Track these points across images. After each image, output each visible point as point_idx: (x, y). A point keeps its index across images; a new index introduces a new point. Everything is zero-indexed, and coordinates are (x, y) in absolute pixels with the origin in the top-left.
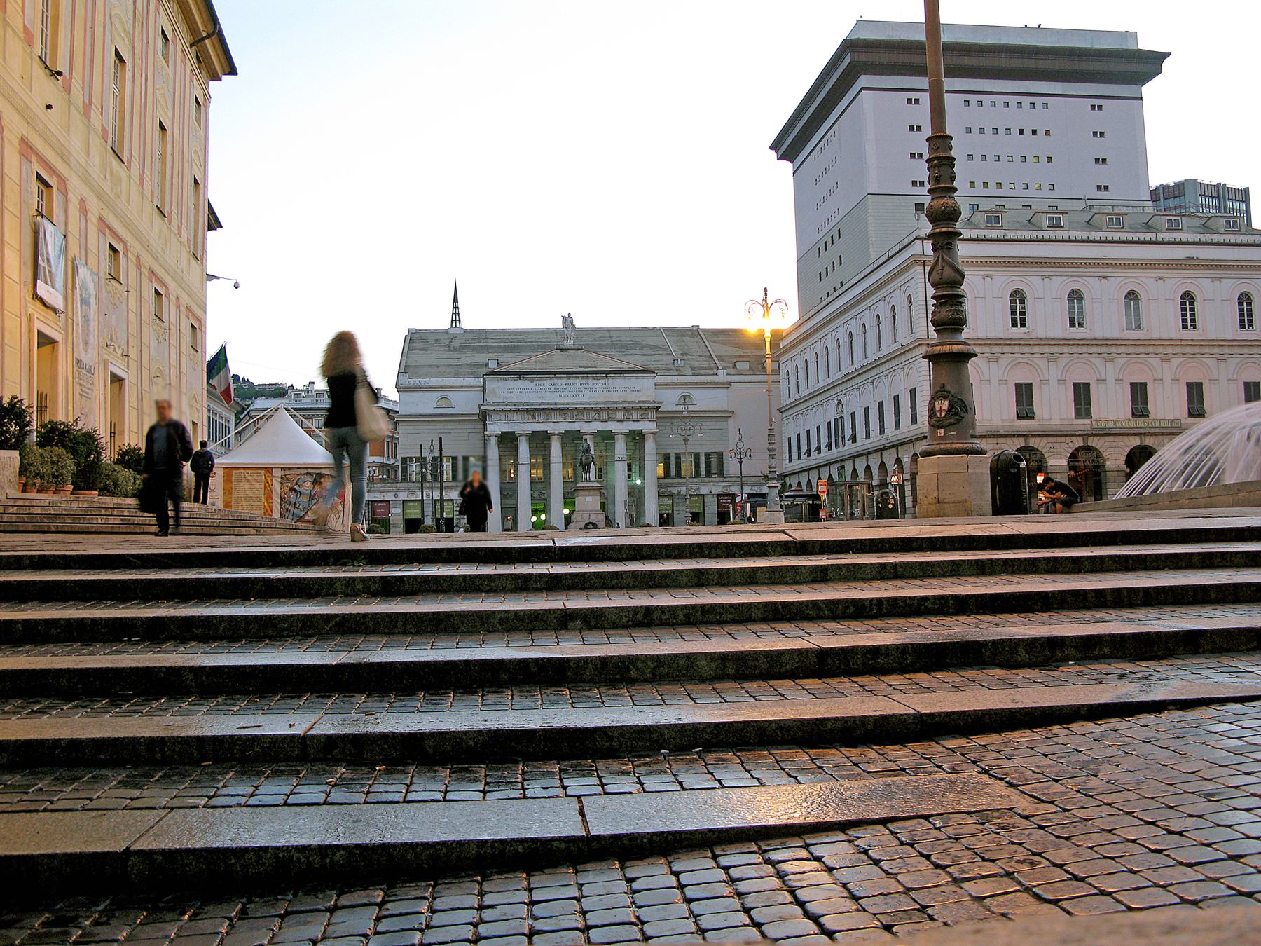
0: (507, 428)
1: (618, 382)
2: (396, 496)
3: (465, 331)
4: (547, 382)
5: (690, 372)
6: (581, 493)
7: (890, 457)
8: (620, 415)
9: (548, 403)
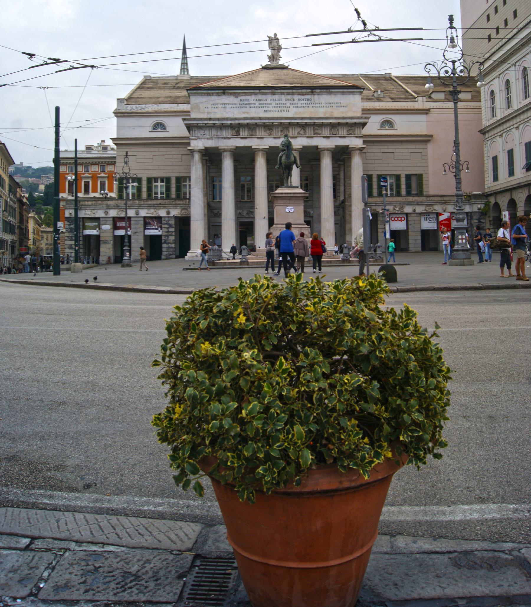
0: (210, 144)
1: (325, 98)
3: (192, 78)
4: (252, 99)
5: (390, 100)
6: (280, 202)
7: (503, 202)
8: (326, 132)
9: (252, 119)
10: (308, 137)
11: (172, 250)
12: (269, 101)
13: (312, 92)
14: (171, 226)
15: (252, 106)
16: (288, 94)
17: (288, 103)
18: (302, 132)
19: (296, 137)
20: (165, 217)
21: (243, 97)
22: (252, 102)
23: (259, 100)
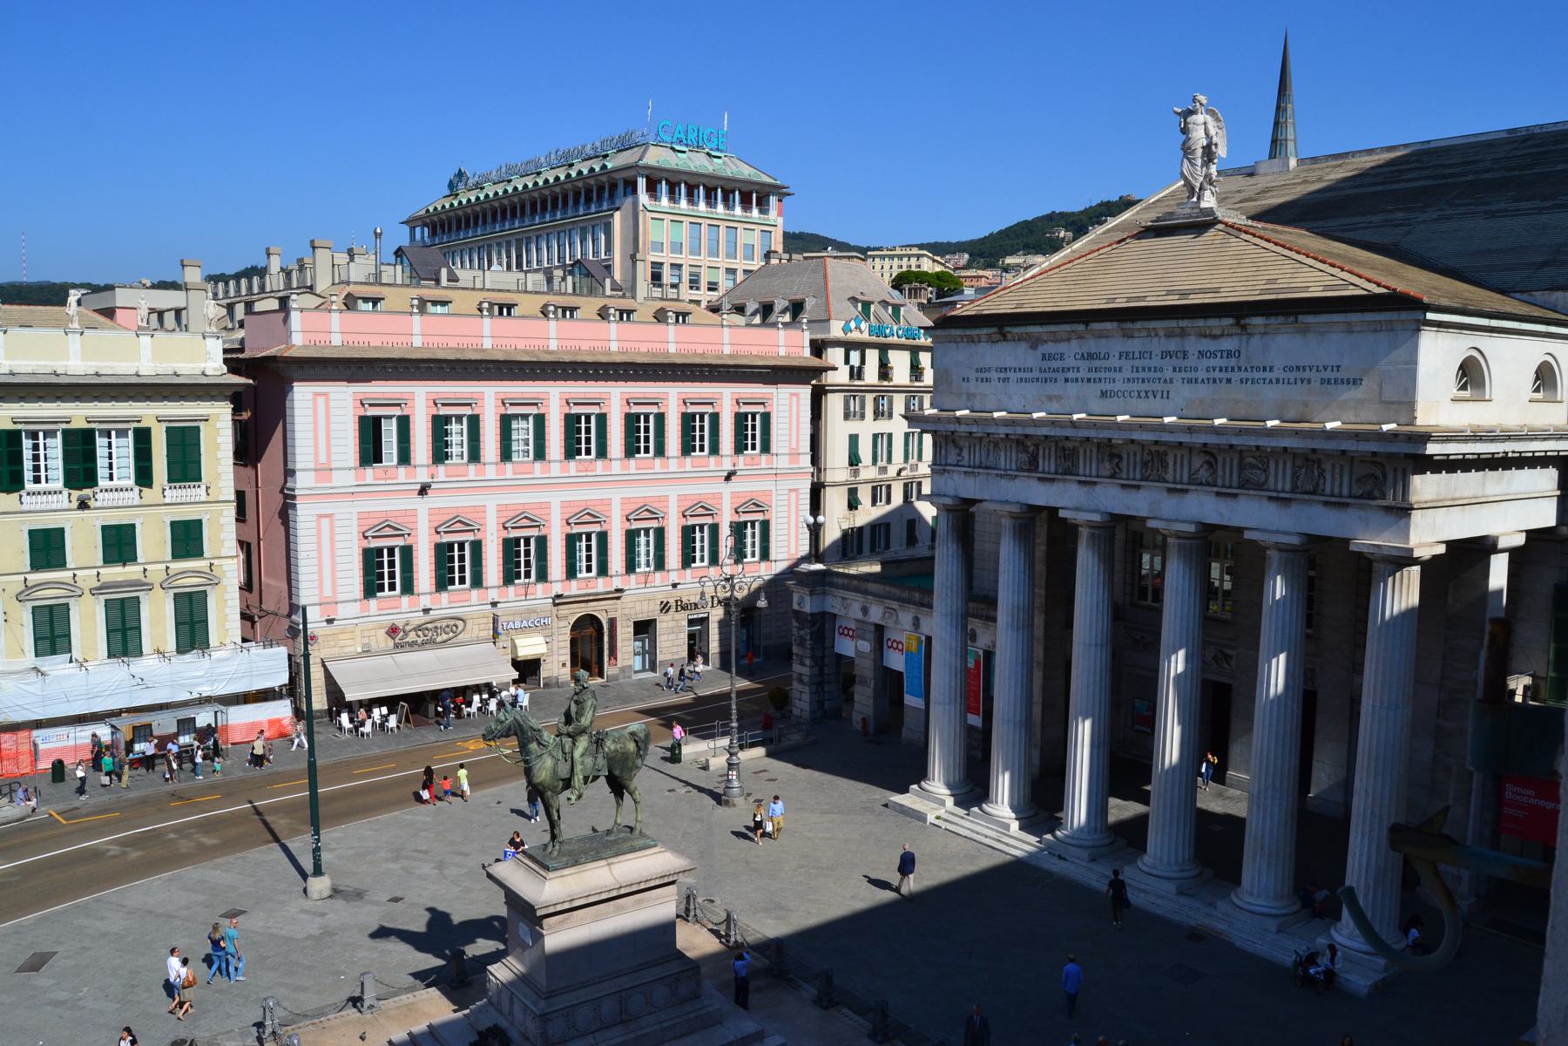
10: (1218, 494)
12: (1114, 362)
13: (1244, 327)
15: (1070, 375)
16: (1170, 335)
17: (1168, 364)
18: (1204, 474)
21: (1049, 348)
22: (1070, 362)
23: (1091, 356)
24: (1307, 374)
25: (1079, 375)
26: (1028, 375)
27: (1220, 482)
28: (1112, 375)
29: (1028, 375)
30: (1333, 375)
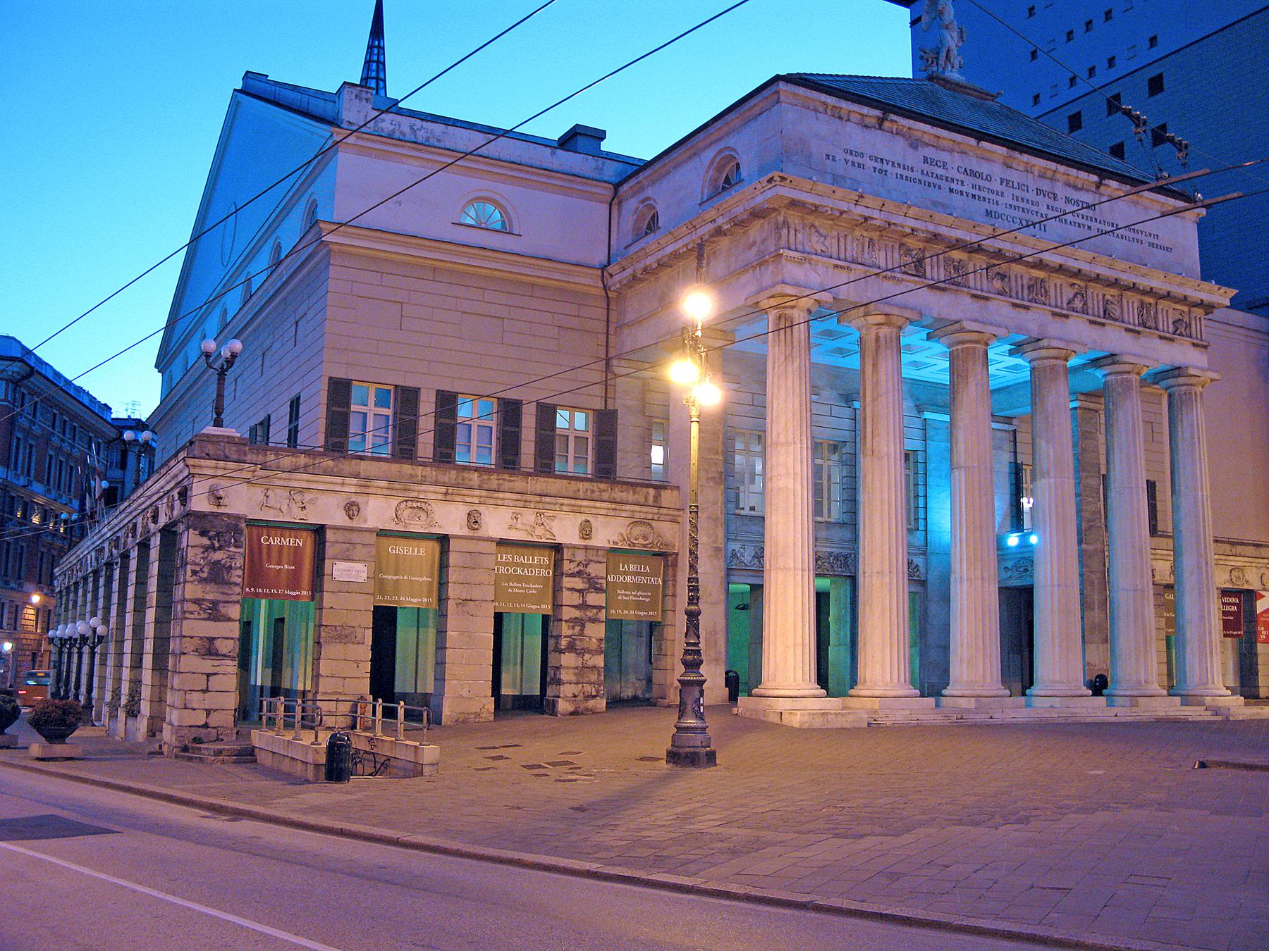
2: (351, 509)
10: (1092, 322)
11: (594, 677)
13: (1098, 187)
14: (594, 586)
15: (954, 186)
18: (1078, 304)
19: (1067, 316)
20: (574, 547)
21: (930, 152)
22: (953, 173)
23: (973, 174)
24: (1139, 236)
25: (964, 189)
26: (909, 174)
27: (1090, 311)
28: (994, 197)
29: (909, 174)
30: (1155, 241)
